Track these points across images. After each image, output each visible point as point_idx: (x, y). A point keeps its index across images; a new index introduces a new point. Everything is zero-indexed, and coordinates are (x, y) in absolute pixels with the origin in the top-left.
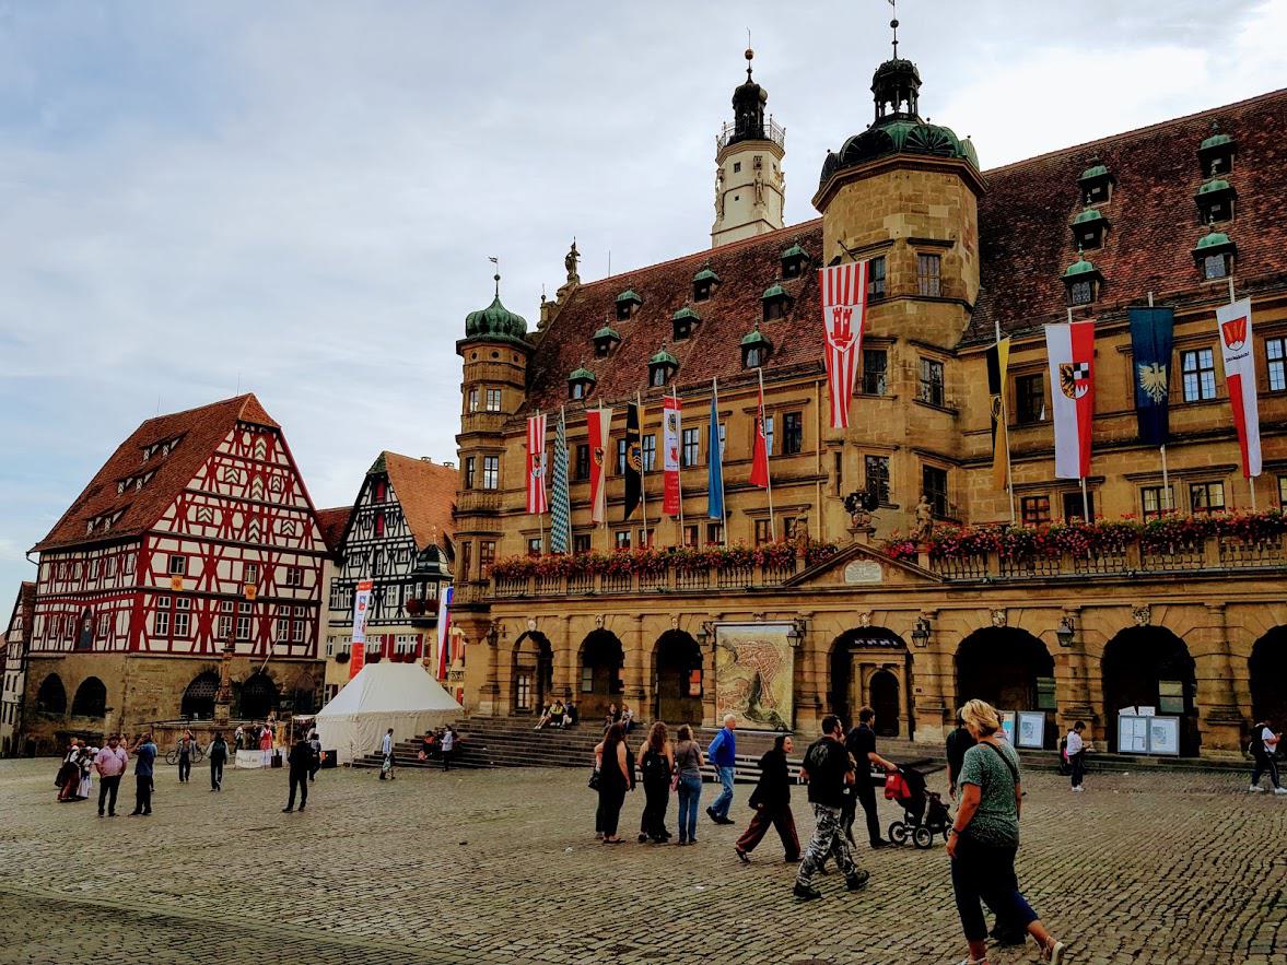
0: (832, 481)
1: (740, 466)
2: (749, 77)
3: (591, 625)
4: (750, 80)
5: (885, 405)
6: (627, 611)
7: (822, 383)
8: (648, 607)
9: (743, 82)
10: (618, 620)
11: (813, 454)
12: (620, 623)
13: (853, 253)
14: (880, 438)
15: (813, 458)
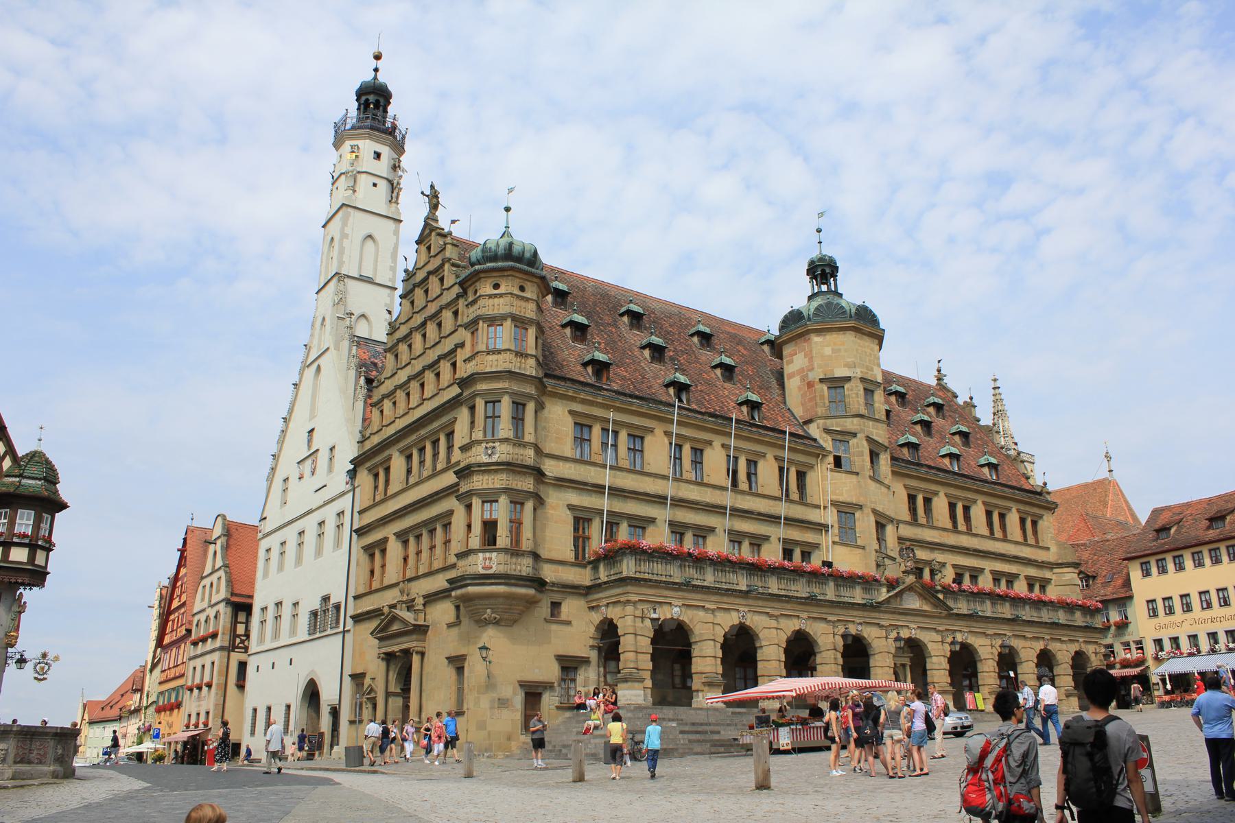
0: (836, 531)
1: (774, 502)
2: (376, 75)
3: (732, 619)
4: (375, 78)
5: (884, 490)
6: (768, 610)
7: (824, 456)
8: (787, 609)
9: (369, 77)
10: (757, 618)
11: (818, 507)
12: (756, 621)
13: (863, 380)
14: (883, 509)
15: (818, 510)
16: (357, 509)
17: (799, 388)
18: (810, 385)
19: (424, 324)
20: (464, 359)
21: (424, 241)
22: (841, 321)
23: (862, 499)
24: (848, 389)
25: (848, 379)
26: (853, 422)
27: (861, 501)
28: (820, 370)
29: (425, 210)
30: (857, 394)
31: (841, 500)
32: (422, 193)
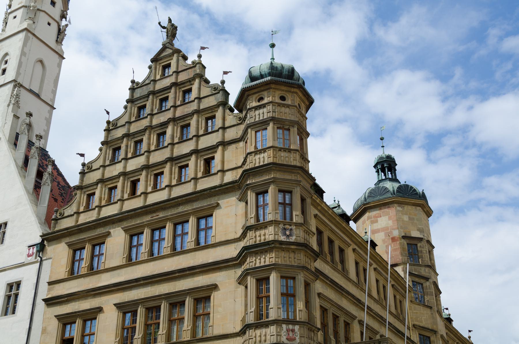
16: (45, 278)
17: (384, 241)
18: (393, 239)
19: (164, 124)
20: (248, 151)
21: (161, 59)
22: (416, 199)
23: (435, 327)
24: (421, 247)
25: (420, 239)
26: (425, 270)
27: (435, 328)
28: (401, 230)
29: (162, 37)
30: (426, 251)
31: (421, 326)
32: (159, 23)
